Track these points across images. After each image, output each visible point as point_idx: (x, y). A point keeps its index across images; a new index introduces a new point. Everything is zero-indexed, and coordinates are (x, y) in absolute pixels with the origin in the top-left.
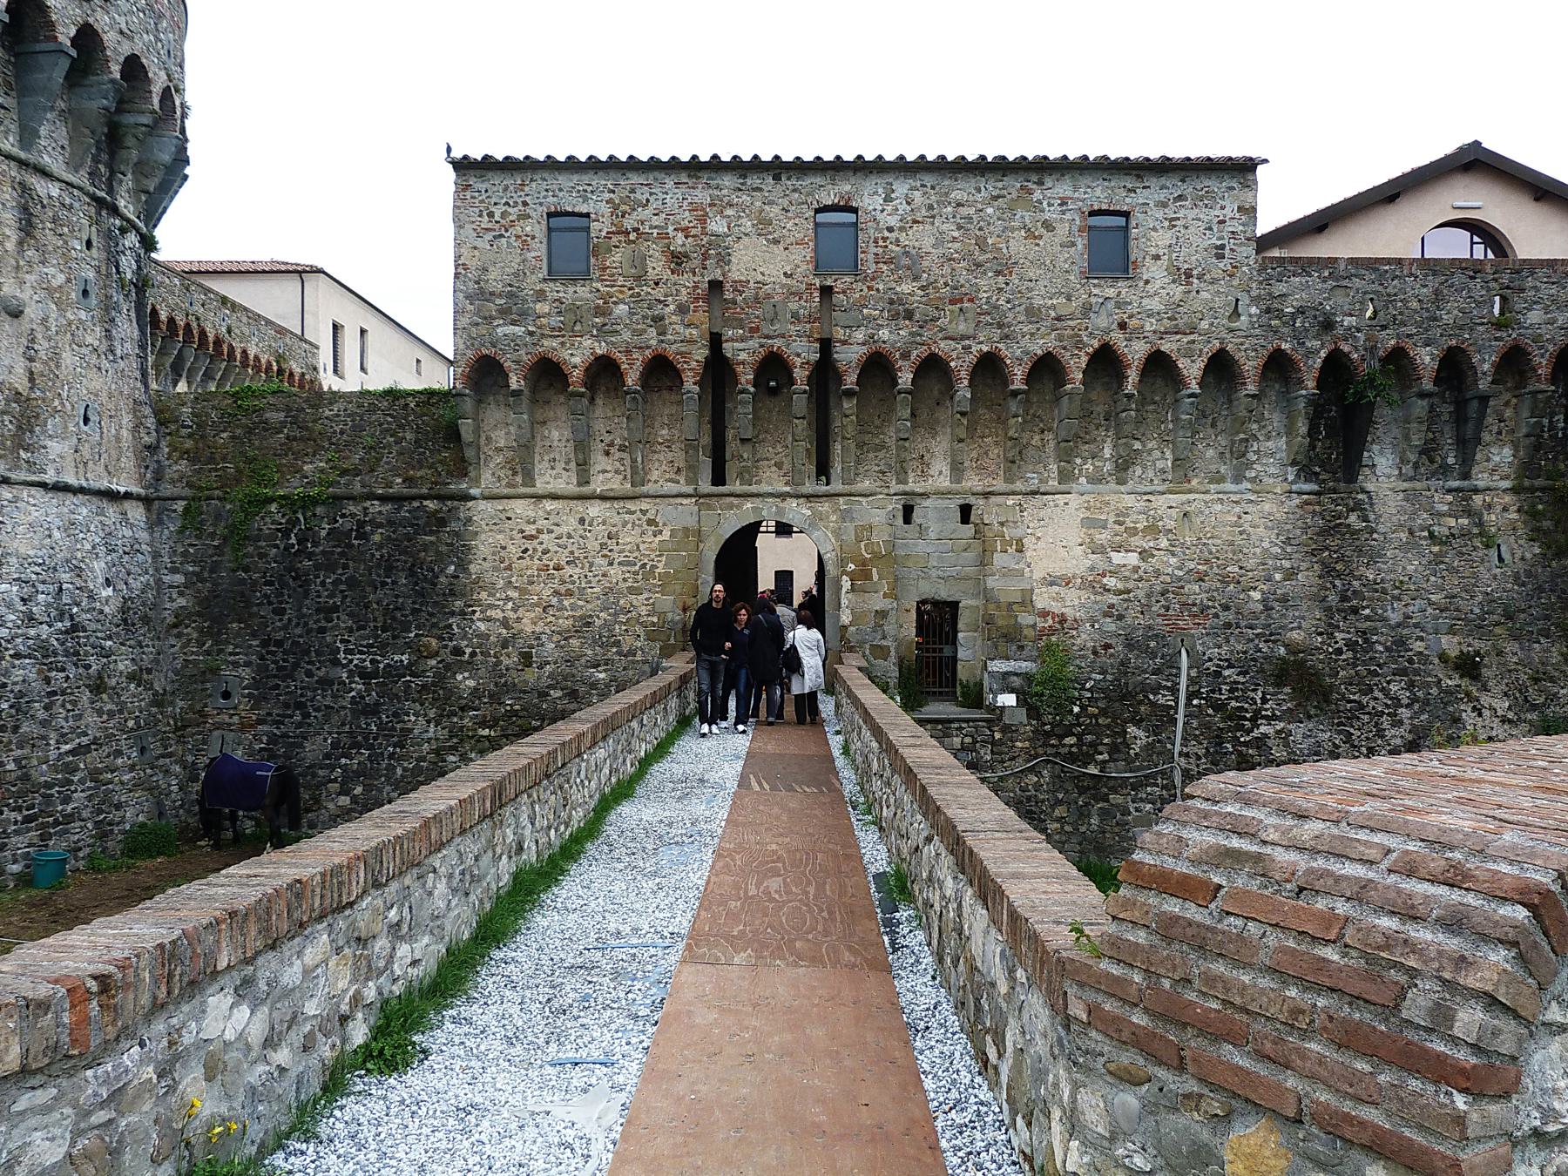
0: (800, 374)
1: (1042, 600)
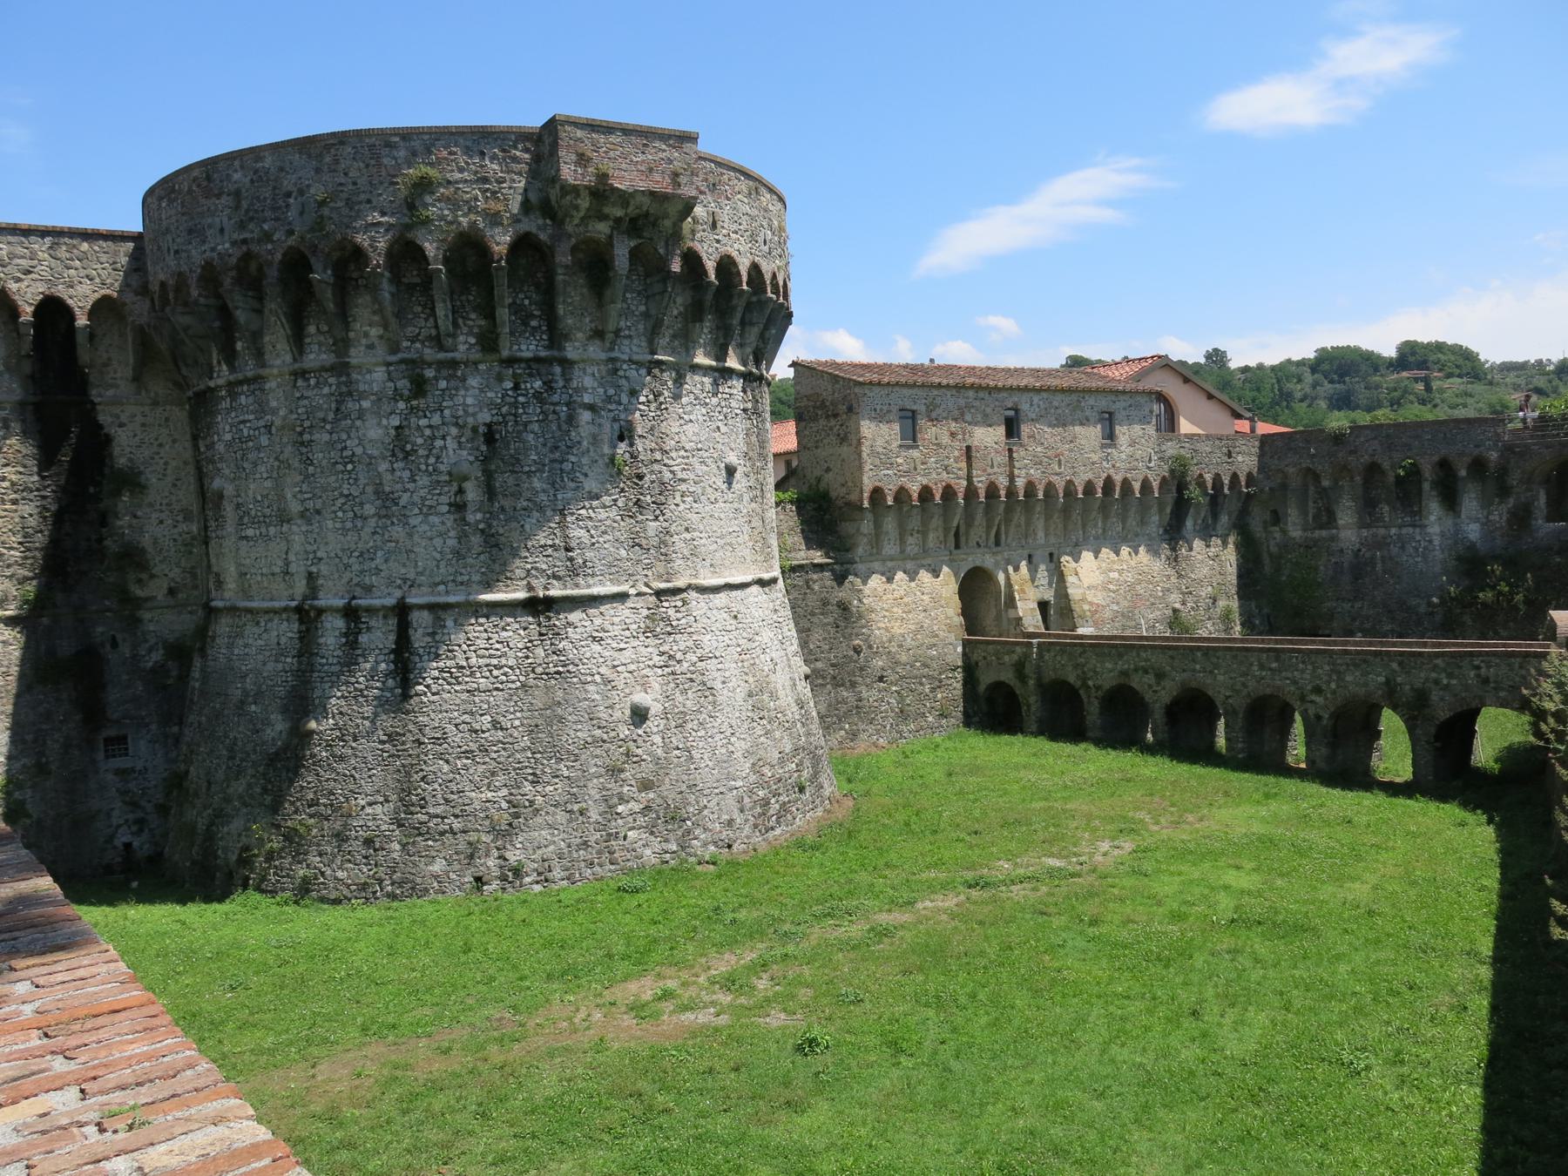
0: (1003, 493)
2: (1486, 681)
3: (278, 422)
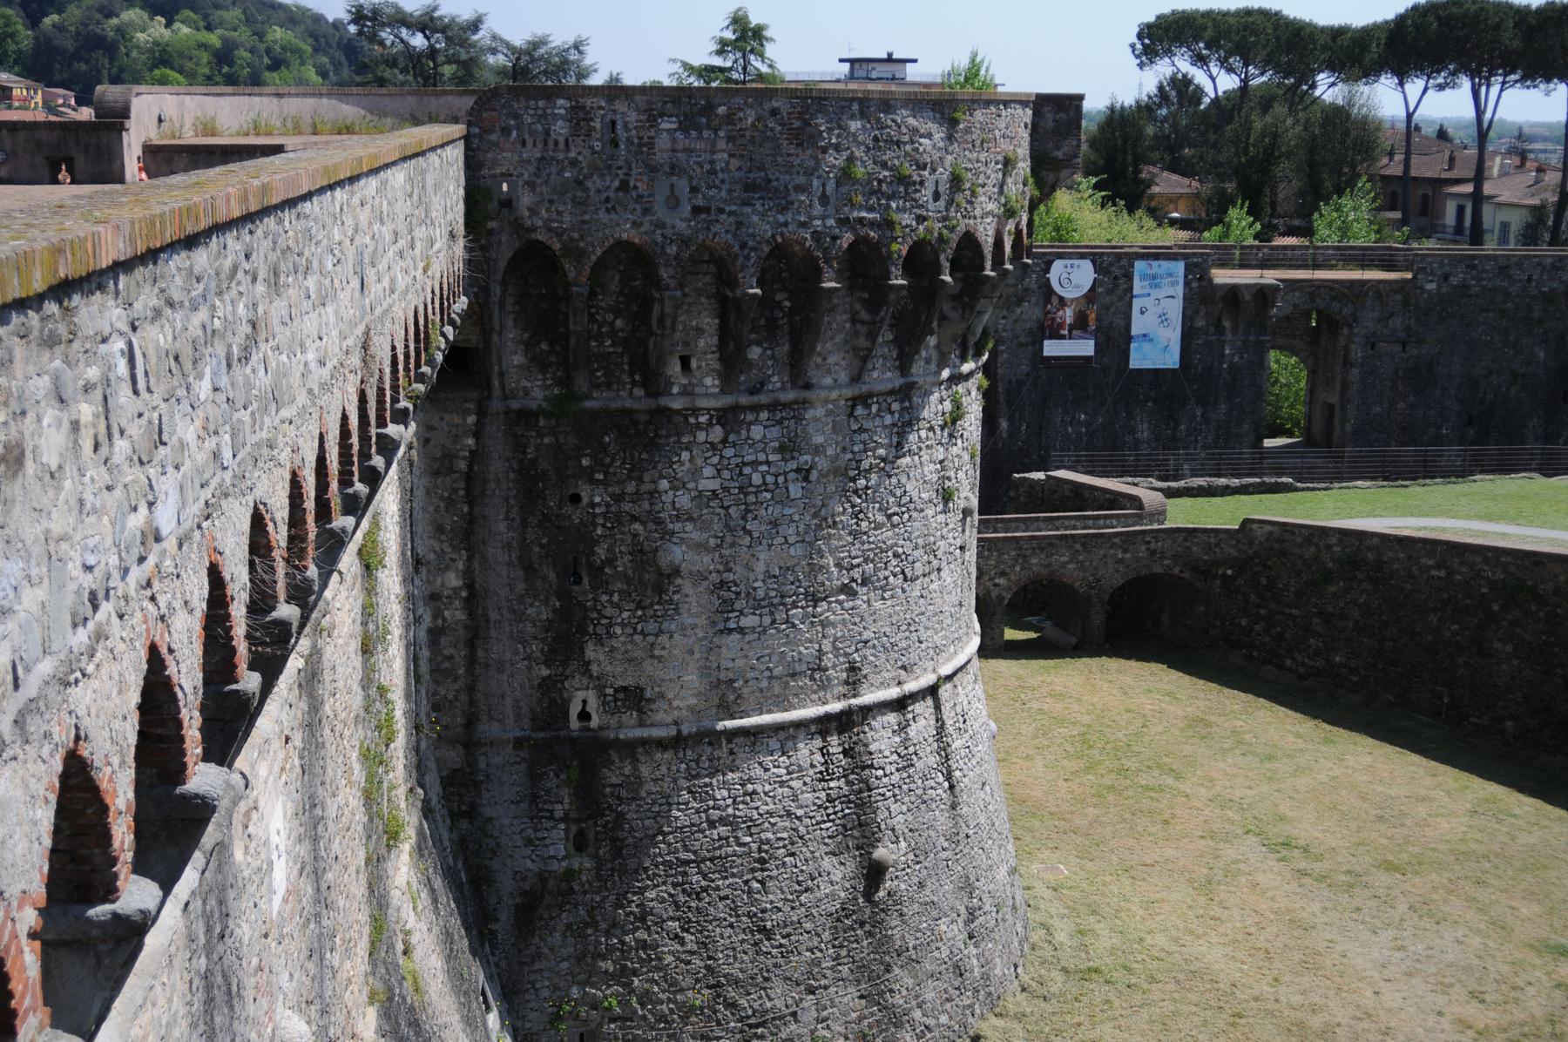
2: (1153, 553)
3: (822, 463)
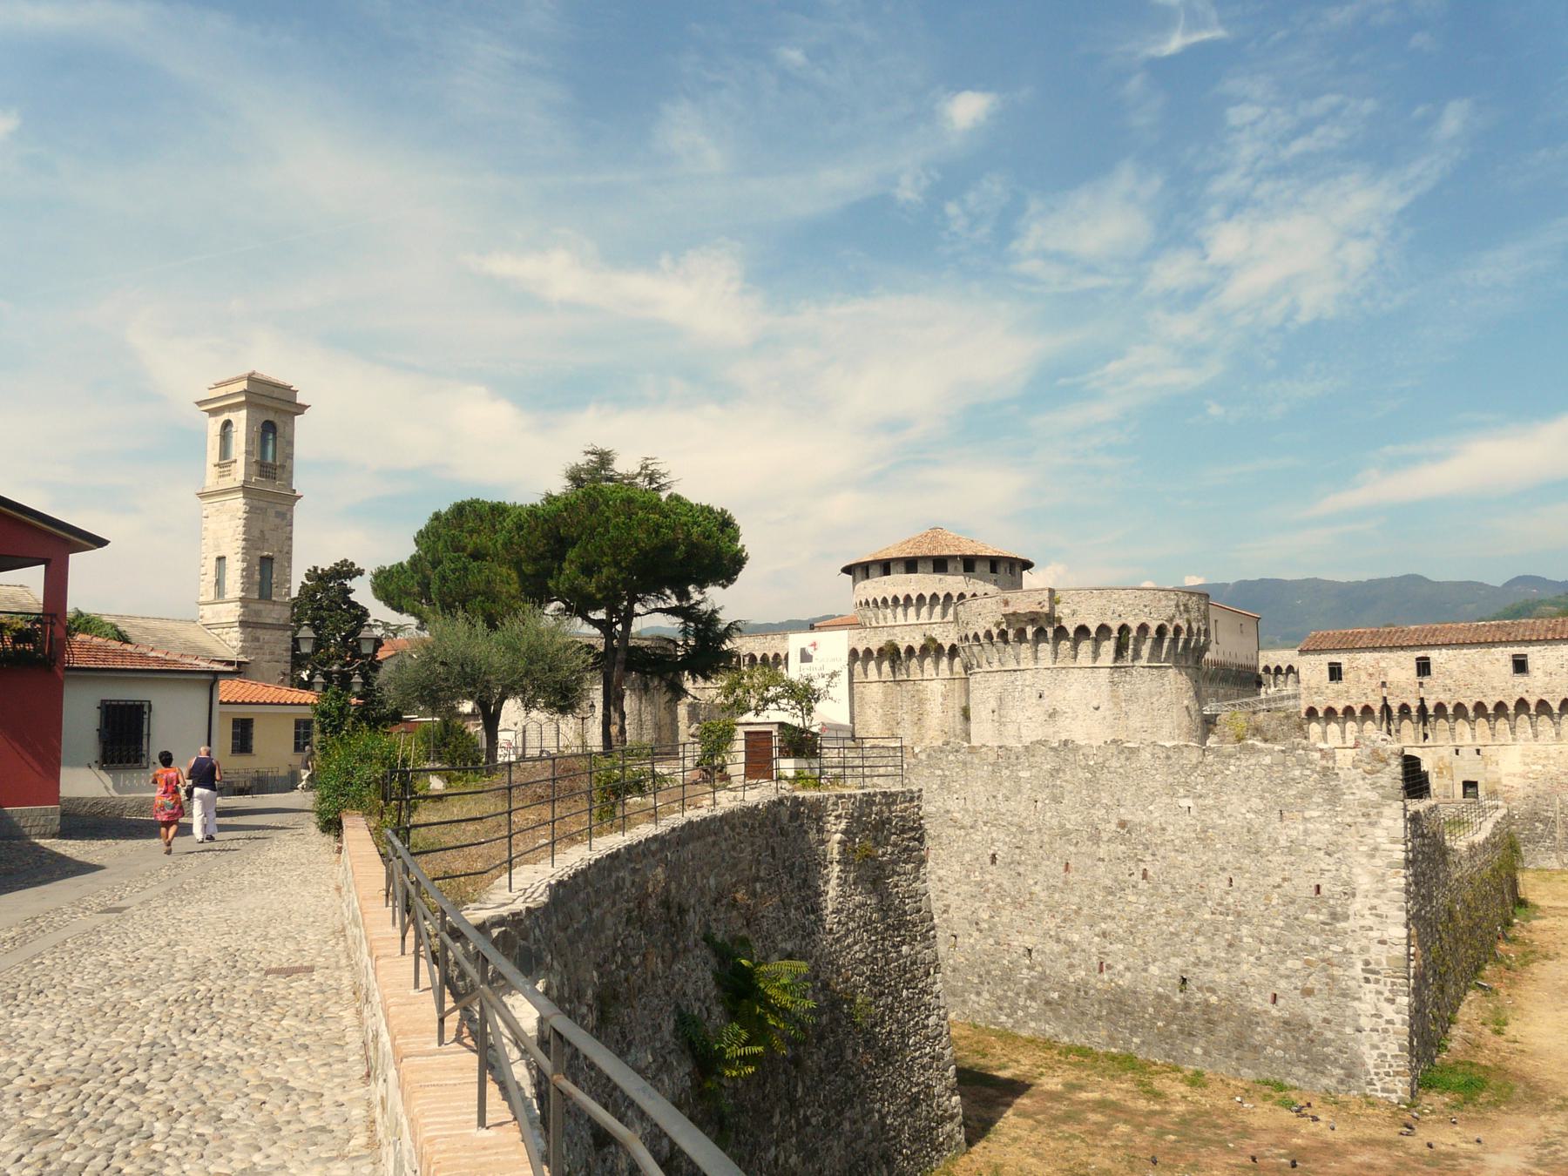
0: (1414, 710)
1: (1504, 781)
